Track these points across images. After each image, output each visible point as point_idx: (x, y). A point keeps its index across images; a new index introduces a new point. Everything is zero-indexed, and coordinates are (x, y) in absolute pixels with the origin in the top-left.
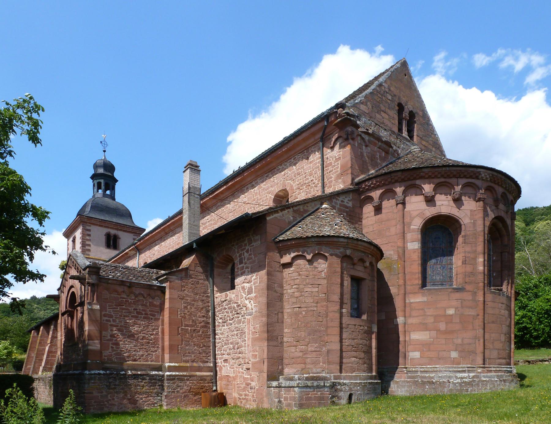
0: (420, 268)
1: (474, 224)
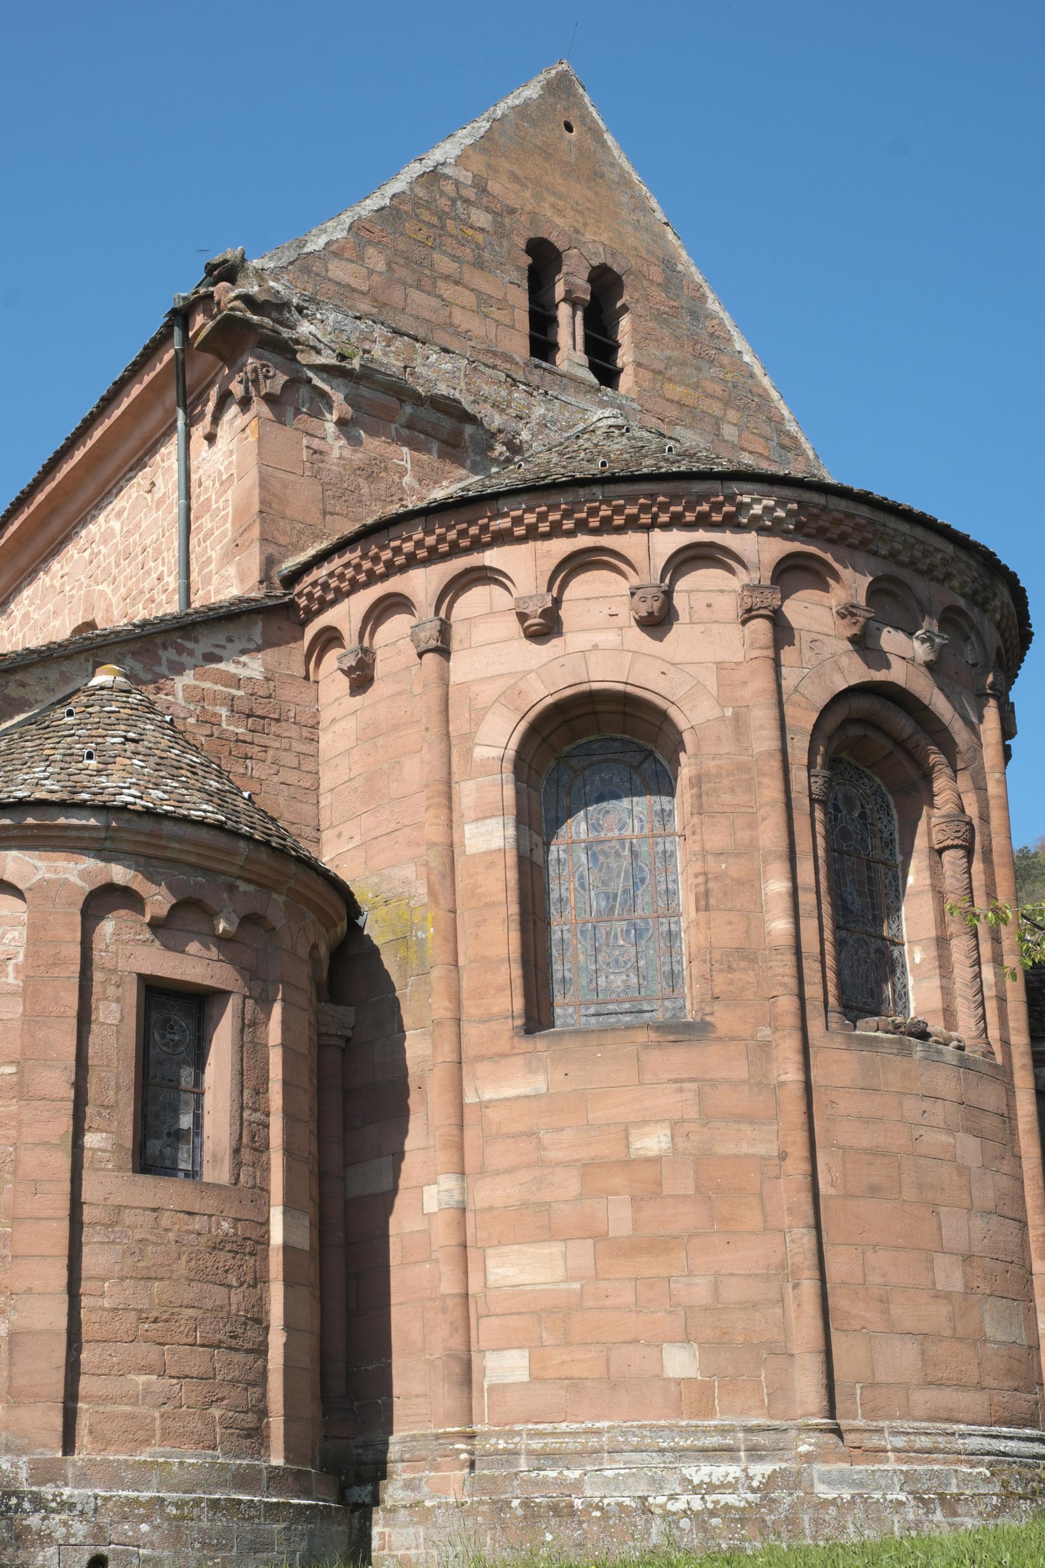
0: (515, 936)
1: (739, 723)
